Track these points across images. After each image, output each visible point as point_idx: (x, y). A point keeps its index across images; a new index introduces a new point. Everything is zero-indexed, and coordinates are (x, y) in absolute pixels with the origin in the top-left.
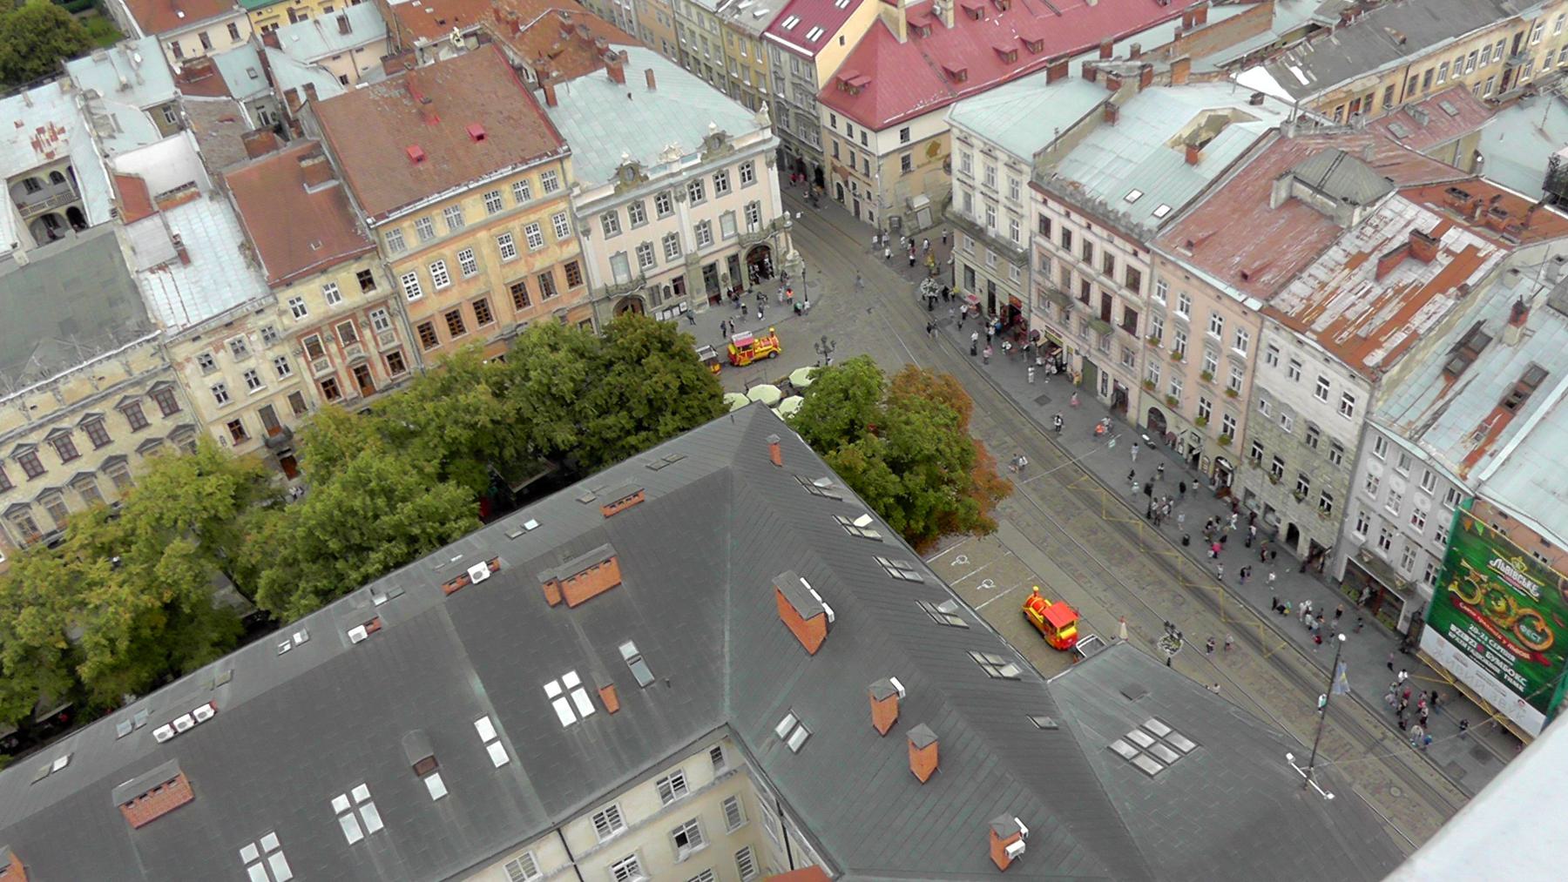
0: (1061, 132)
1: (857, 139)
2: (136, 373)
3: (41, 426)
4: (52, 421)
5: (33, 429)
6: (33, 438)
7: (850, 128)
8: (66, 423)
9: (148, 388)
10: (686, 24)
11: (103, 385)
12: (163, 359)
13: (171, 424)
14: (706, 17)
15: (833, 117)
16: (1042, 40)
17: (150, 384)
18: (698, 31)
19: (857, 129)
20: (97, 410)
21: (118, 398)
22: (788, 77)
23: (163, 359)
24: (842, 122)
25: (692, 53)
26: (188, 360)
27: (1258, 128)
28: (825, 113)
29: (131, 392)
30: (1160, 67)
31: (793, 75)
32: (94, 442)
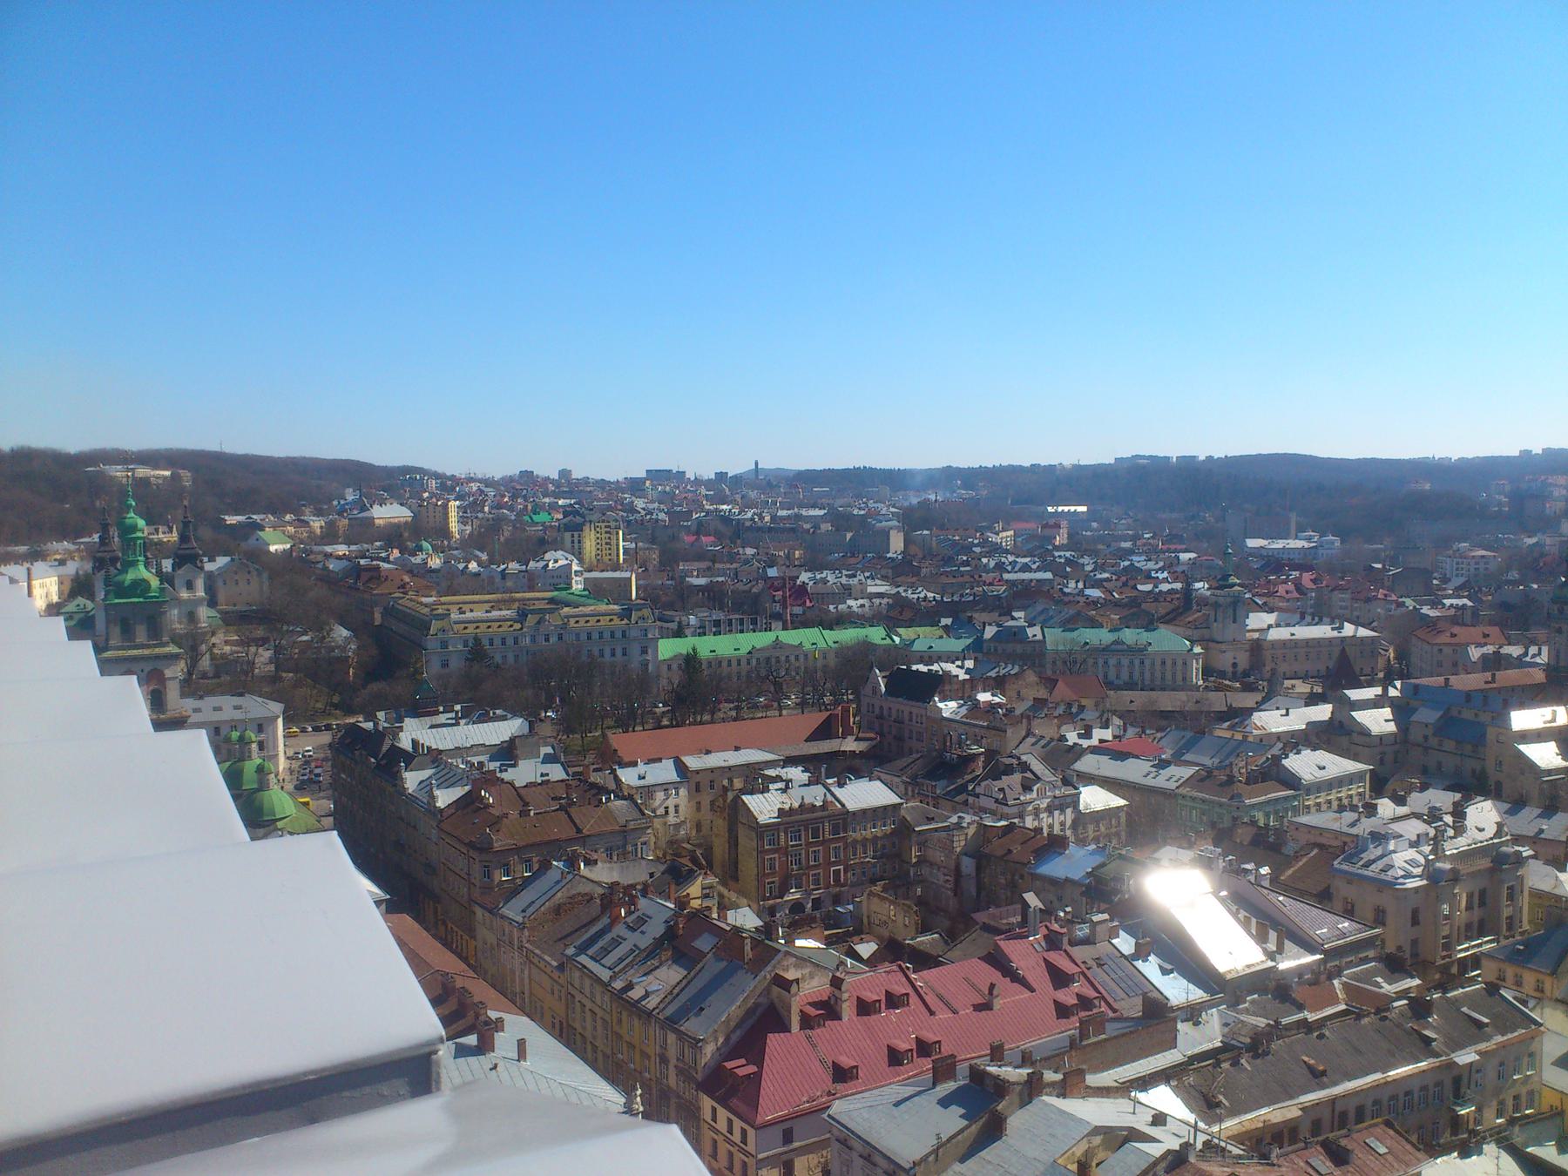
0: (944, 1138)
1: (737, 1137)
7: (730, 1122)
10: (578, 997)
14: (598, 989)
15: (714, 1110)
16: (939, 1042)
18: (589, 1004)
19: (738, 1124)
22: (673, 1062)
24: (723, 1114)
25: (580, 1030)
27: (1155, 1150)
28: (707, 1103)
30: (1050, 1076)
31: (678, 1059)
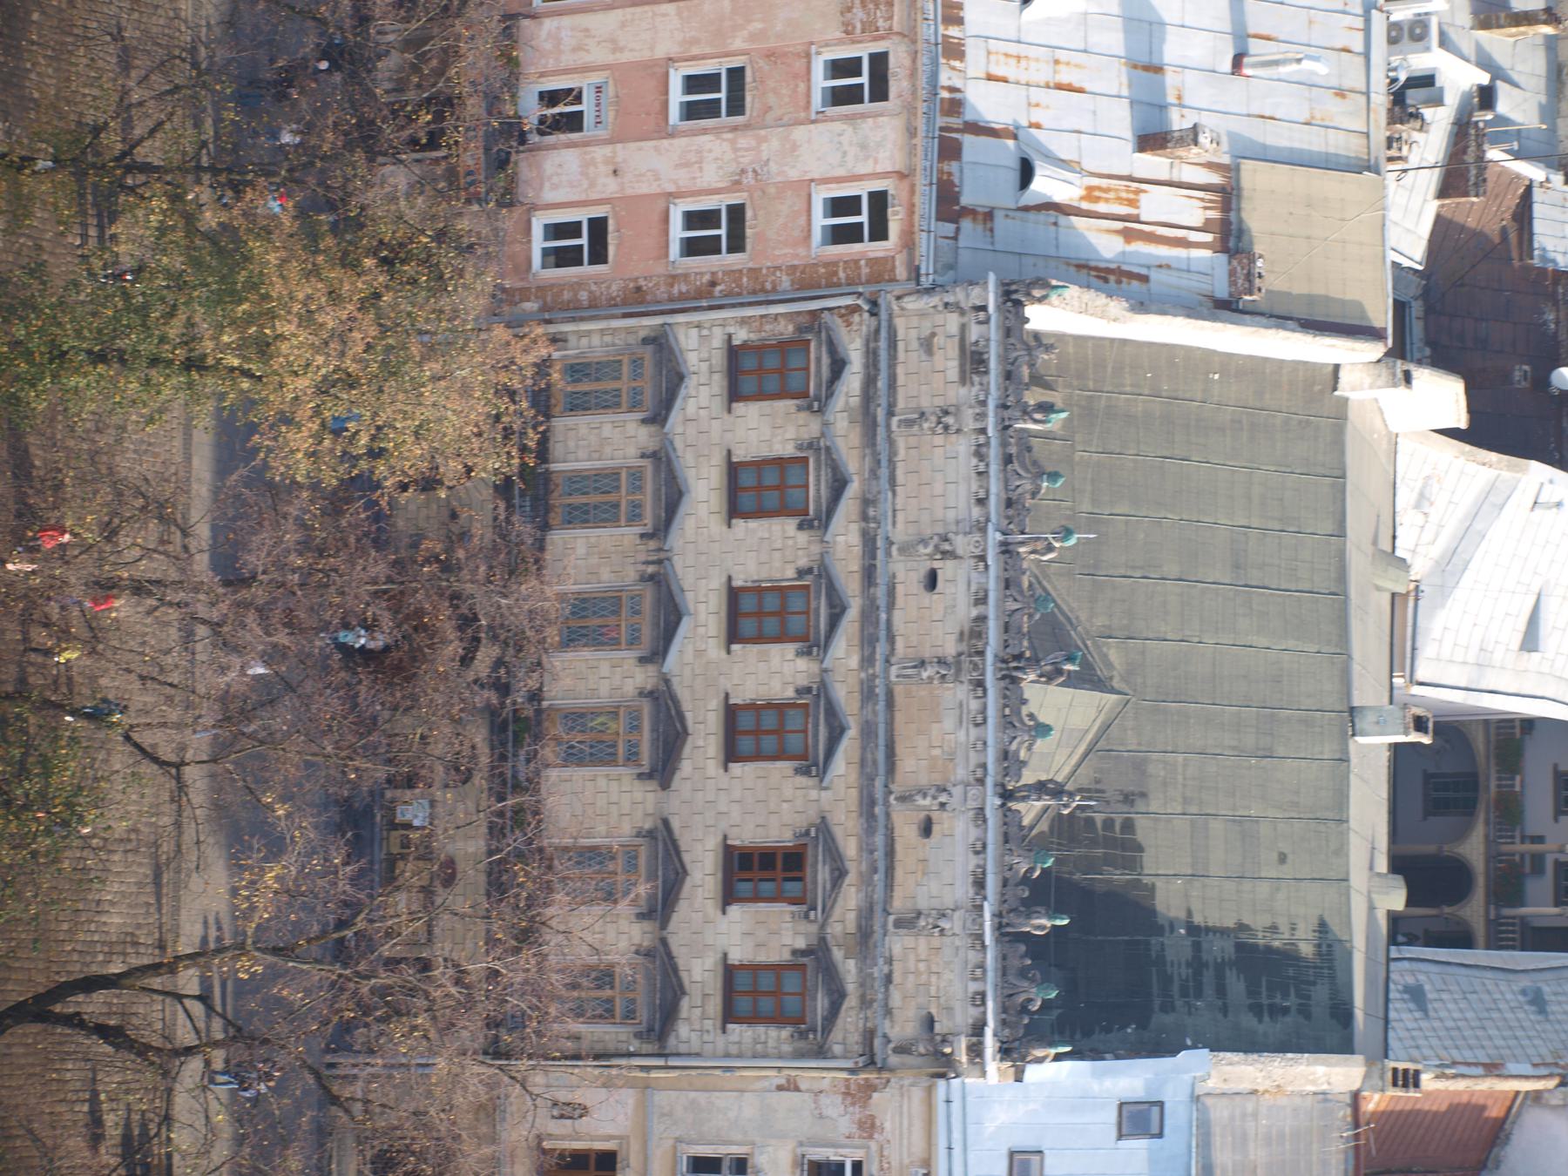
2: (897, 943)
3: (869, 575)
4: (869, 615)
5: (869, 541)
6: (845, 535)
8: (844, 652)
9: (838, 954)
11: (906, 832)
12: (902, 1050)
13: (700, 973)
17: (849, 969)
20: (843, 765)
21: (850, 848)
23: (902, 1050)
26: (869, 1127)
29: (850, 899)
32: (752, 707)
